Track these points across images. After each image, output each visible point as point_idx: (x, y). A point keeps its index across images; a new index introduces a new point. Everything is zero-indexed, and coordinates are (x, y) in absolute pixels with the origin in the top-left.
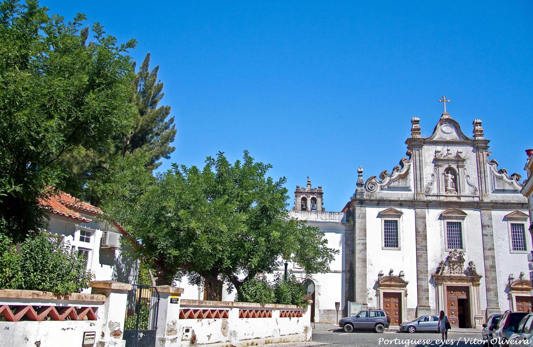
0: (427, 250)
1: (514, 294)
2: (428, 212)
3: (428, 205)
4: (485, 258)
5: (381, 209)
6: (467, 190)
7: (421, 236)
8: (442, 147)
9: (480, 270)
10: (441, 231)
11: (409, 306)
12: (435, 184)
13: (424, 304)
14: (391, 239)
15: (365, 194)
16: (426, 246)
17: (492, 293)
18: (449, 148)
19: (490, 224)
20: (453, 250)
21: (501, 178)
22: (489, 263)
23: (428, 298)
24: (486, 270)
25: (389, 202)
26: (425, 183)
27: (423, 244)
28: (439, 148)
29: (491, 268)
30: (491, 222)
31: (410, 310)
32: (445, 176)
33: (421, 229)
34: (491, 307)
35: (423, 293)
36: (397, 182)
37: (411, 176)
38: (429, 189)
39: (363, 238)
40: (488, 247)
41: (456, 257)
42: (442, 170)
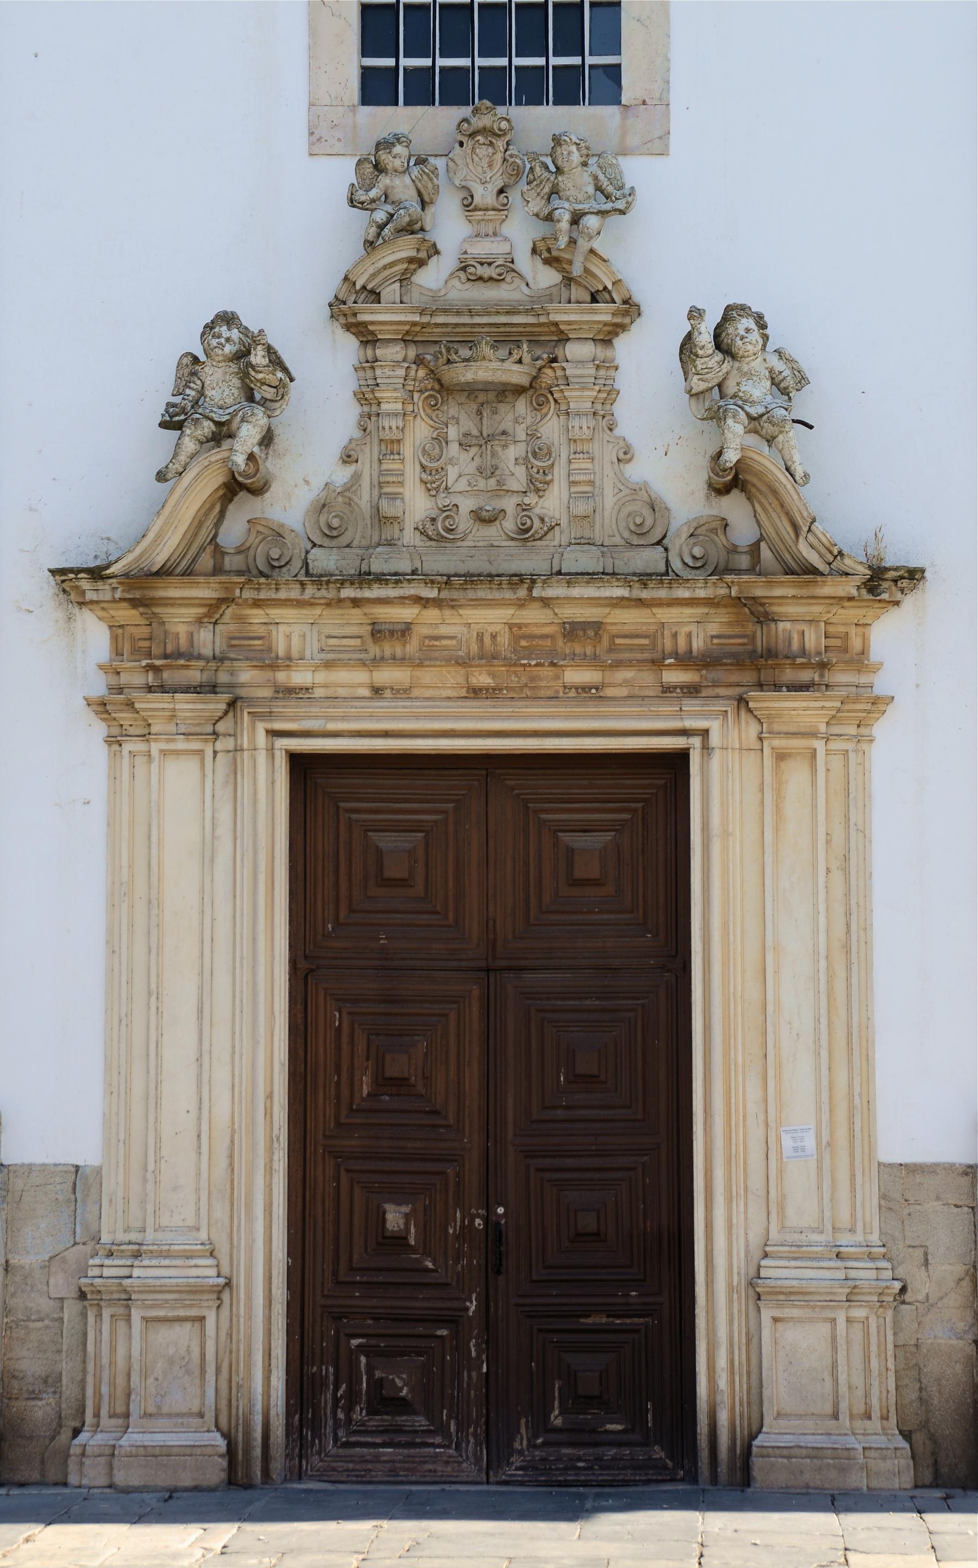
20: (433, 123)
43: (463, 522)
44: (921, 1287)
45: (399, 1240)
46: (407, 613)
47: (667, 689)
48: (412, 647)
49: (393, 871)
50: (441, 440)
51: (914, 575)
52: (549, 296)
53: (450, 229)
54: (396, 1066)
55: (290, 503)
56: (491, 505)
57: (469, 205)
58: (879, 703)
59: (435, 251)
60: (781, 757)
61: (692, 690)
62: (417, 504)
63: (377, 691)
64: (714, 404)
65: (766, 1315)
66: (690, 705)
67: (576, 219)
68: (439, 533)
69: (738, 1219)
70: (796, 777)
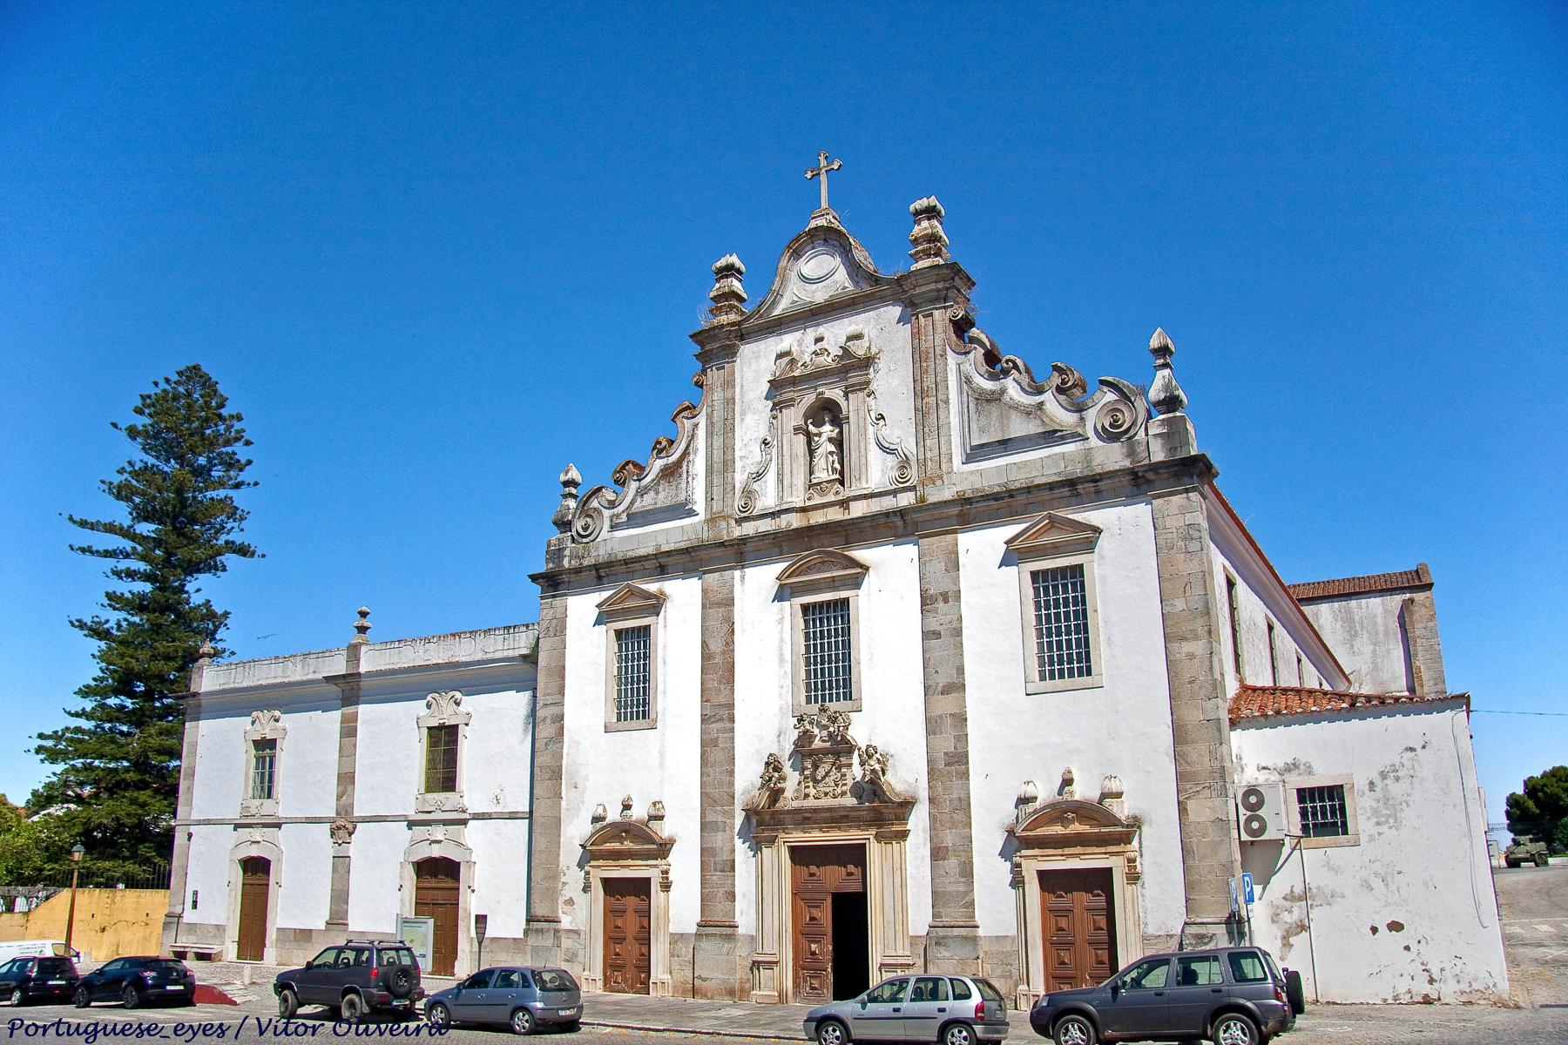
1: (1033, 865)
2: (743, 578)
3: (741, 553)
5: (606, 594)
6: (876, 472)
7: (718, 668)
8: (798, 334)
9: (908, 773)
10: (782, 640)
12: (771, 476)
14: (634, 701)
15: (567, 552)
16: (731, 706)
17: (952, 863)
18: (821, 330)
21: (995, 398)
22: (947, 744)
23: (732, 896)
26: (740, 478)
27: (722, 699)
28: (788, 341)
29: (950, 765)
30: (956, 581)
31: (677, 938)
32: (808, 435)
33: (716, 646)
34: (946, 920)
35: (716, 877)
36: (652, 493)
37: (699, 464)
38: (748, 494)
39: (556, 698)
40: (941, 680)
41: (825, 733)
42: (793, 417)
45: (813, 953)
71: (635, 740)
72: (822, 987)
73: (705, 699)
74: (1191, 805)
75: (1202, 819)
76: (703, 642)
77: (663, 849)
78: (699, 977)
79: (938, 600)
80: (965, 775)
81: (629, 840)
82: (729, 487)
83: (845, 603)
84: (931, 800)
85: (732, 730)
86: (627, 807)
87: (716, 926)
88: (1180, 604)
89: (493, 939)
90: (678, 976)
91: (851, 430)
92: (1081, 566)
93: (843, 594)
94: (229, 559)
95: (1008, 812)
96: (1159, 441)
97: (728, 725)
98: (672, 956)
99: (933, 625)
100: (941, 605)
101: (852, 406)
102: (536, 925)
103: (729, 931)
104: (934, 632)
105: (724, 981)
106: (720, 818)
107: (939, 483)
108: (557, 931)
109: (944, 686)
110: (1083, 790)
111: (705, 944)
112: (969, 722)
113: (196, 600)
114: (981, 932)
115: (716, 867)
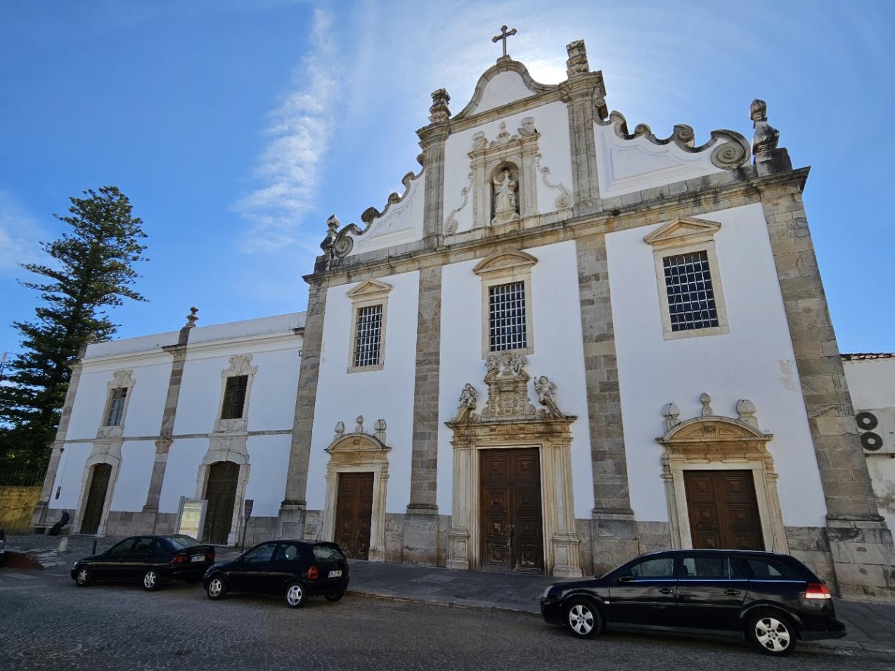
0: (438, 363)
1: (681, 465)
4: (590, 364)
7: (429, 328)
11: (390, 509)
13: (424, 501)
14: (368, 350)
15: (329, 263)
16: (437, 354)
17: (608, 464)
19: (600, 271)
23: (433, 486)
24: (591, 398)
25: (370, 265)
26: (446, 213)
27: (431, 350)
29: (604, 392)
30: (605, 267)
32: (493, 185)
33: (427, 317)
40: (596, 333)
42: (483, 175)
43: (504, 412)
44: (584, 541)
46: (495, 427)
47: (536, 437)
48: (496, 433)
49: (495, 468)
50: (501, 400)
51: (574, 418)
52: (516, 377)
53: (502, 368)
54: (497, 501)
55: (479, 411)
56: (508, 409)
57: (504, 364)
58: (571, 439)
59: (499, 371)
60: (555, 448)
61: (539, 437)
62: (498, 409)
63: (491, 439)
64: (539, 391)
65: (555, 545)
66: (539, 440)
67: (518, 366)
68: (500, 414)
69: (550, 528)
70: (557, 451)
71: (368, 375)
72: (503, 556)
73: (419, 351)
74: (820, 422)
75: (832, 433)
76: (419, 313)
77: (385, 448)
78: (407, 547)
79: (591, 280)
80: (617, 398)
81: (361, 444)
82: (440, 218)
83: (521, 284)
84: (591, 417)
85: (437, 370)
86: (360, 421)
87: (422, 508)
88: (793, 273)
89: (257, 518)
90: (391, 546)
91: (525, 181)
92: (705, 252)
93: (519, 279)
94: (126, 300)
95: (656, 426)
96: (766, 165)
97: (435, 366)
98: (387, 530)
99: (588, 295)
100: (593, 283)
101: (525, 164)
102: (288, 507)
103: (431, 512)
104: (588, 300)
105: (426, 551)
106: (427, 430)
107: (590, 204)
108: (305, 511)
109: (598, 334)
110: (721, 409)
111: (413, 522)
112: (618, 360)
113: (99, 318)
114: (638, 517)
115: (424, 464)
